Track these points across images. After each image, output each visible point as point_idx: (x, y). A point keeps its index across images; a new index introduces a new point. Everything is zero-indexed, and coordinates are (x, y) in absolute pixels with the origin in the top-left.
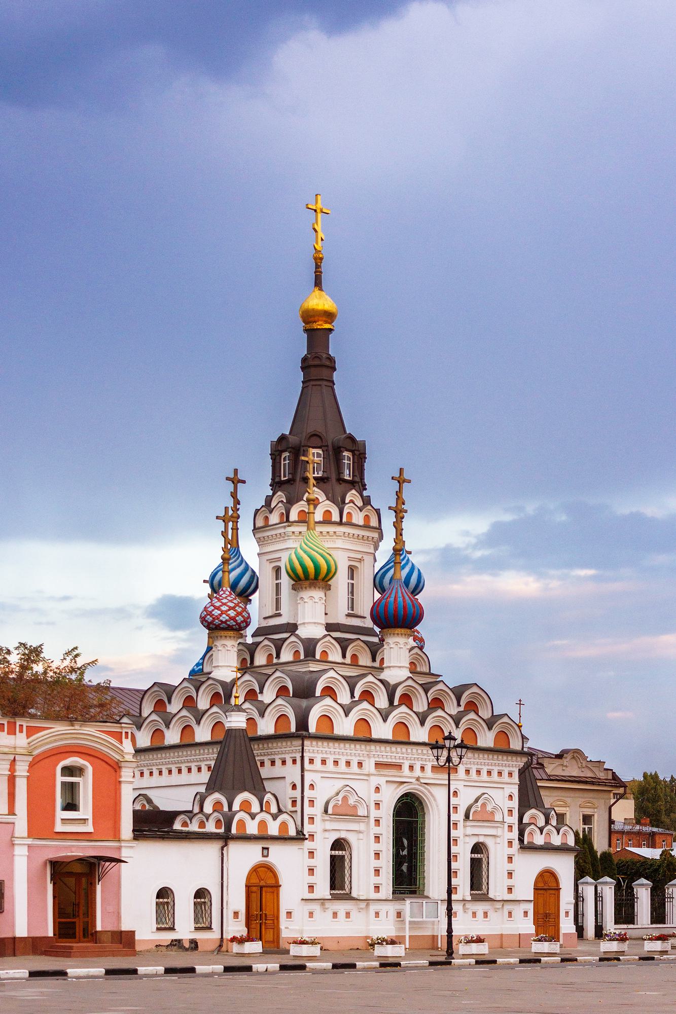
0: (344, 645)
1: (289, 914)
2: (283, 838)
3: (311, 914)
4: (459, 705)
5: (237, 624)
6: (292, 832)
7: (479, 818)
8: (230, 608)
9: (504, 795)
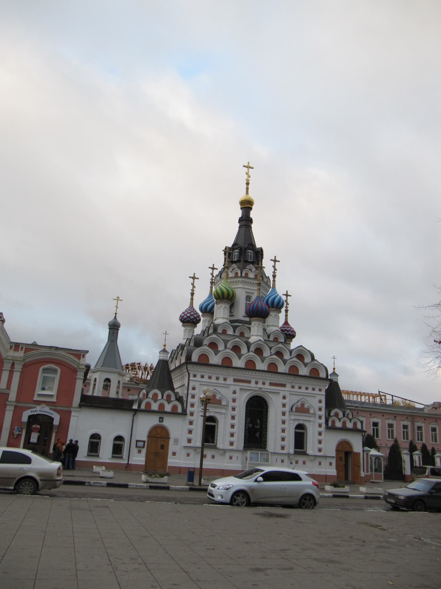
0: (235, 328)
1: (174, 454)
2: (174, 413)
3: (188, 455)
4: (291, 354)
5: (191, 320)
6: (180, 410)
8: (188, 313)
9: (316, 399)
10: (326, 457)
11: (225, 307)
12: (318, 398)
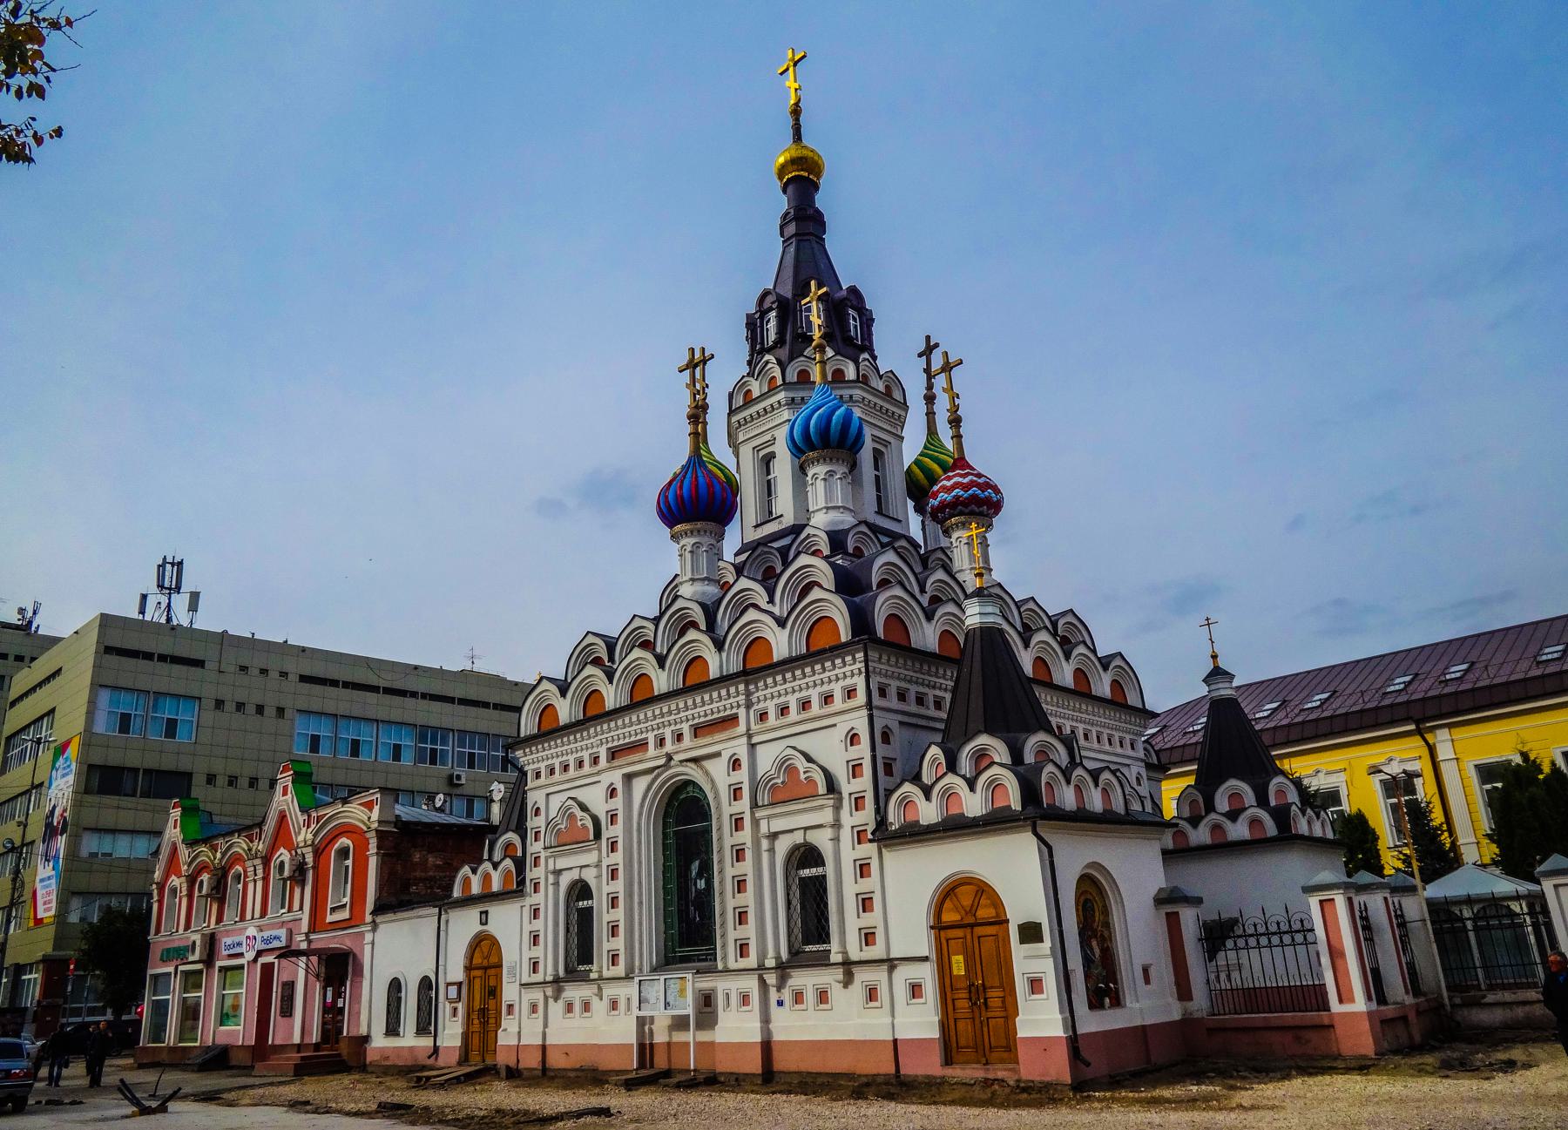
7: (781, 797)
10: (891, 963)
12: (843, 726)
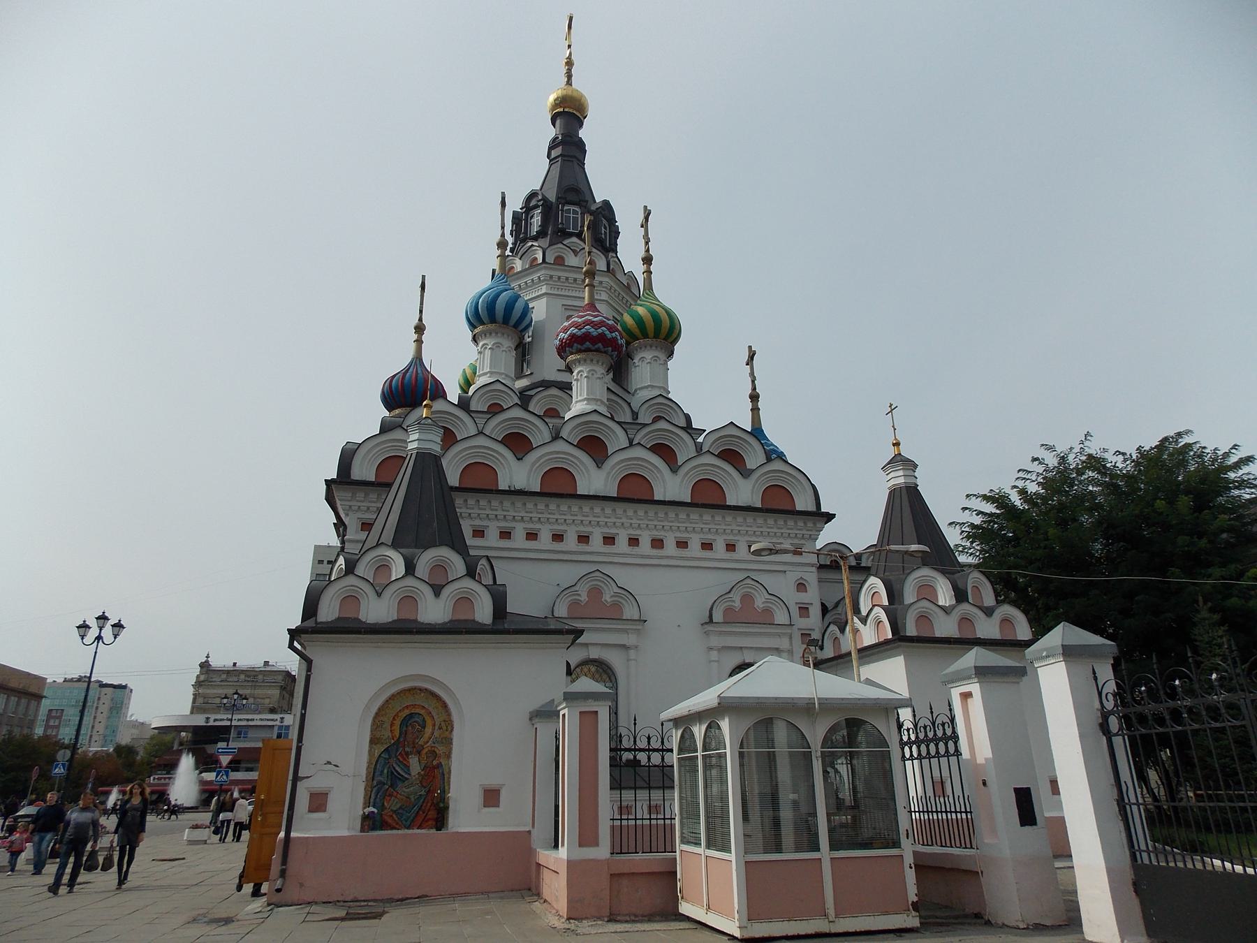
11: (498, 345)
